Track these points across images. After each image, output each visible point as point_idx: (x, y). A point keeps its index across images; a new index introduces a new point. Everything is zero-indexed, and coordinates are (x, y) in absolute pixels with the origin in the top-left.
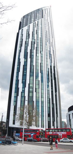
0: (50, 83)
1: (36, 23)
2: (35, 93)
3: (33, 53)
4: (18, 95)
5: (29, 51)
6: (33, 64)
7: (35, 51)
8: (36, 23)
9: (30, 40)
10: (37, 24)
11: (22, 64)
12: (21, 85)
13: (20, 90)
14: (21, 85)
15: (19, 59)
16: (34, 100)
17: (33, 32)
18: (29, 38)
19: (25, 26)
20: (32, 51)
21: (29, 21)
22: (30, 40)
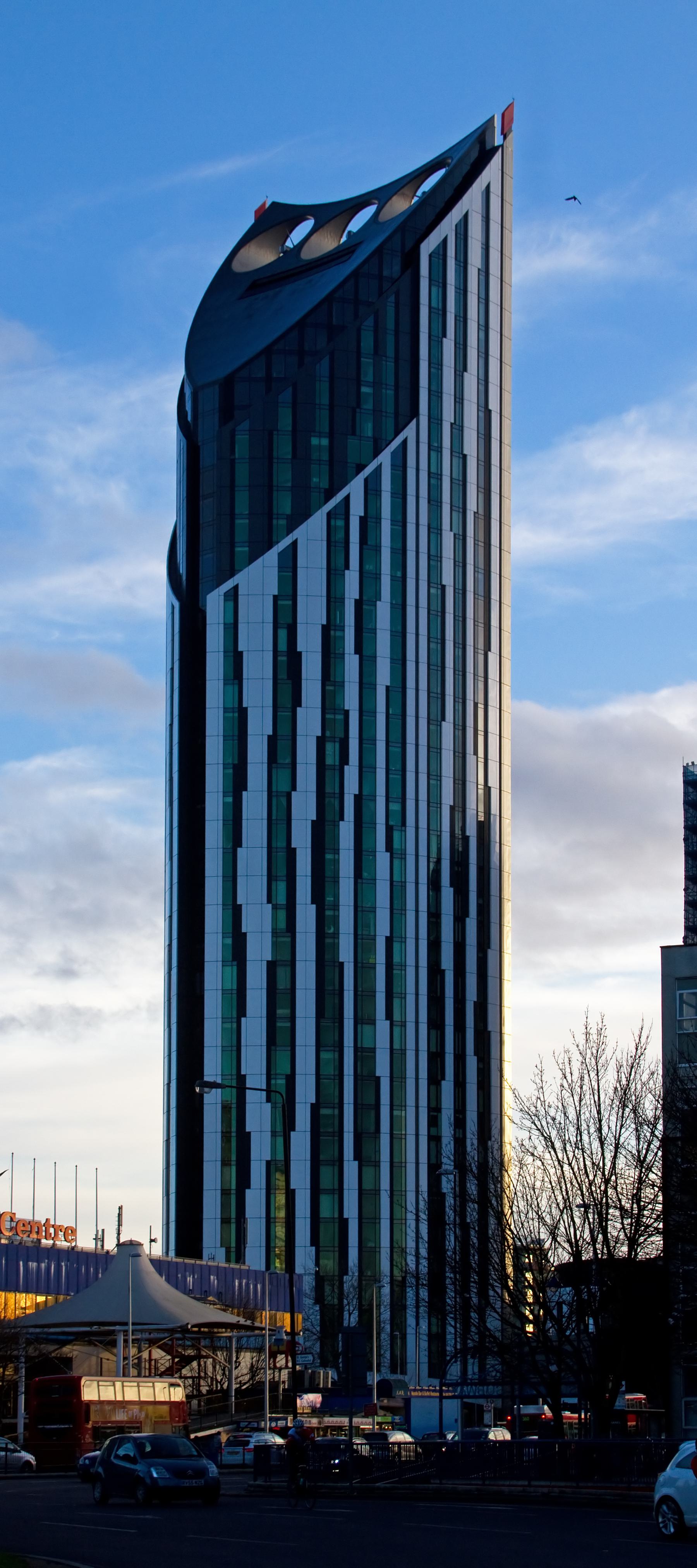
0: (447, 1087)
1: (357, 509)
2: (351, 1168)
3: (336, 851)
4: (244, 1181)
5: (302, 839)
6: (336, 947)
7: (346, 830)
8: (357, 509)
9: (309, 721)
10: (363, 521)
11: (259, 951)
12: (259, 1116)
13: (261, 1150)
14: (259, 1116)
15: (235, 912)
16: (351, 1211)
17: (326, 630)
18: (297, 701)
19: (253, 557)
20: (328, 828)
21: (284, 476)
22: (309, 721)
